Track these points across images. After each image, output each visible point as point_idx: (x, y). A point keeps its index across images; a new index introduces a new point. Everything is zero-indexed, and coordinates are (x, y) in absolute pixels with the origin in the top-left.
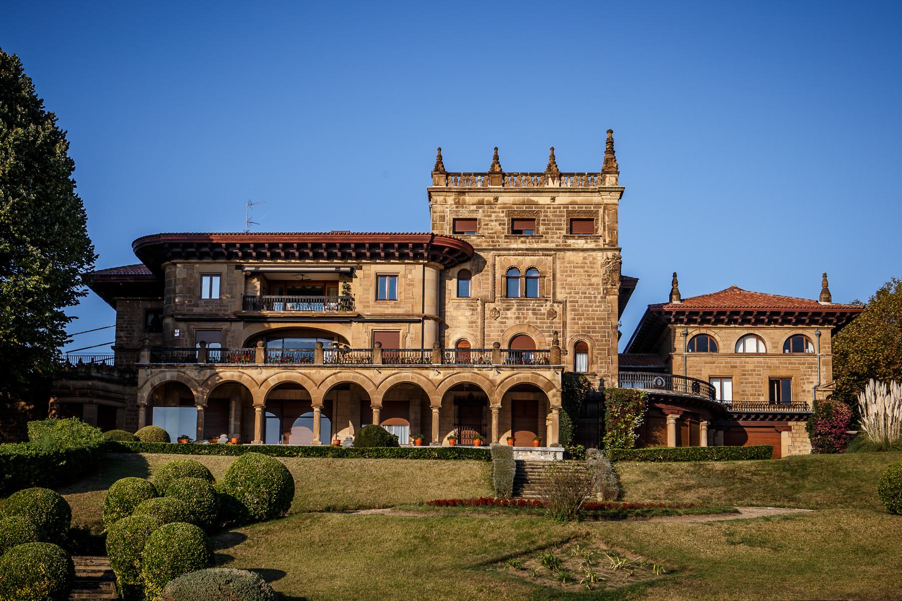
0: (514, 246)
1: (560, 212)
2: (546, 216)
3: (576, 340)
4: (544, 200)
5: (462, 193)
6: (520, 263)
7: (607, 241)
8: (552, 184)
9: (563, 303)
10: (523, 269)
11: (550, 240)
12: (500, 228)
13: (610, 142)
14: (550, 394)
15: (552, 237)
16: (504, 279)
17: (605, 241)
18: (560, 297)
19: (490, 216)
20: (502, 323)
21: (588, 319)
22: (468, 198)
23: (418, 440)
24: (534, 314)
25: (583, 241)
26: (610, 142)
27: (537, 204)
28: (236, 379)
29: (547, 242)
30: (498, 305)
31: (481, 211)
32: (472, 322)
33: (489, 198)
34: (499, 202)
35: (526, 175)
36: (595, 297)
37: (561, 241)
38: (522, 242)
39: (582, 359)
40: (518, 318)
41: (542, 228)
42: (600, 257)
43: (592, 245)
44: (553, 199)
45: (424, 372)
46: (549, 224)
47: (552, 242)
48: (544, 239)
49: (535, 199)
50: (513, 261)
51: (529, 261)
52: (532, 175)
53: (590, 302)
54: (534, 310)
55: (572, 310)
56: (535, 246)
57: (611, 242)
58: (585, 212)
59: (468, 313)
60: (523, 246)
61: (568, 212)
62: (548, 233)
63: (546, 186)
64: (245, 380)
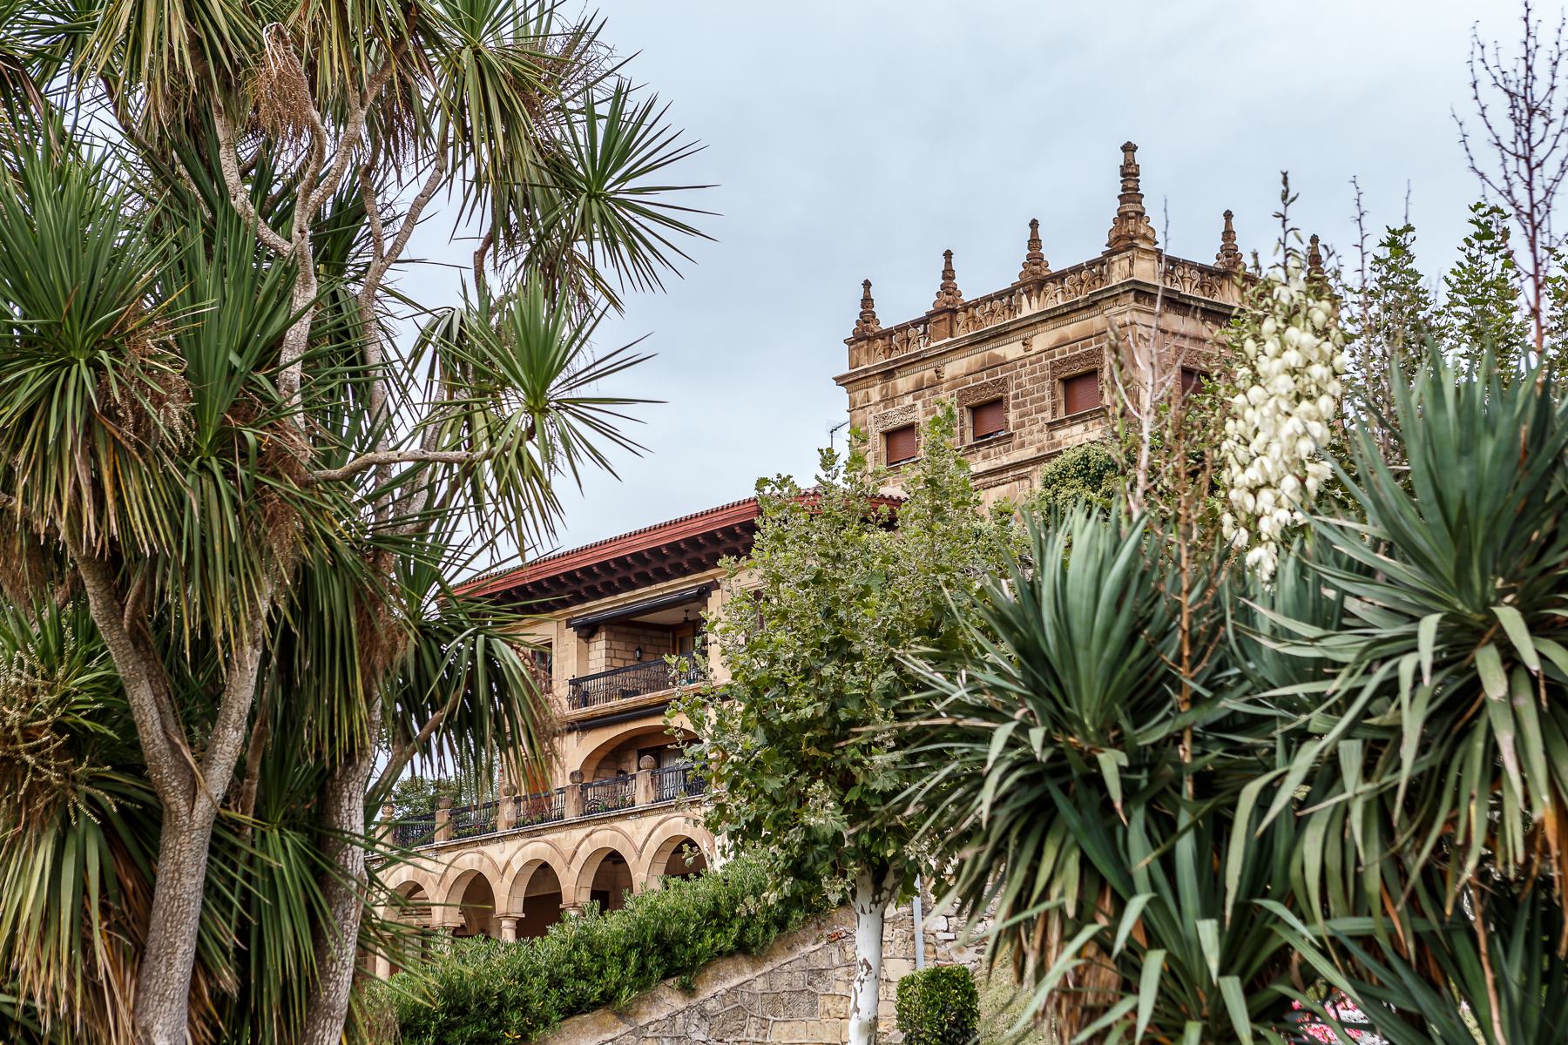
1: (1042, 369)
2: (1019, 386)
4: (1011, 350)
5: (888, 374)
8: (1029, 308)
11: (1027, 439)
13: (1129, 173)
15: (1031, 433)
22: (903, 383)
25: (1081, 427)
26: (1129, 173)
27: (1002, 363)
28: (475, 867)
29: (1022, 445)
31: (919, 403)
33: (929, 373)
34: (947, 376)
37: (1044, 436)
38: (985, 457)
41: (1012, 416)
48: (1017, 441)
49: (998, 351)
52: (999, 296)
56: (1005, 460)
58: (1079, 358)
61: (1054, 367)
62: (1023, 425)
63: (1019, 316)
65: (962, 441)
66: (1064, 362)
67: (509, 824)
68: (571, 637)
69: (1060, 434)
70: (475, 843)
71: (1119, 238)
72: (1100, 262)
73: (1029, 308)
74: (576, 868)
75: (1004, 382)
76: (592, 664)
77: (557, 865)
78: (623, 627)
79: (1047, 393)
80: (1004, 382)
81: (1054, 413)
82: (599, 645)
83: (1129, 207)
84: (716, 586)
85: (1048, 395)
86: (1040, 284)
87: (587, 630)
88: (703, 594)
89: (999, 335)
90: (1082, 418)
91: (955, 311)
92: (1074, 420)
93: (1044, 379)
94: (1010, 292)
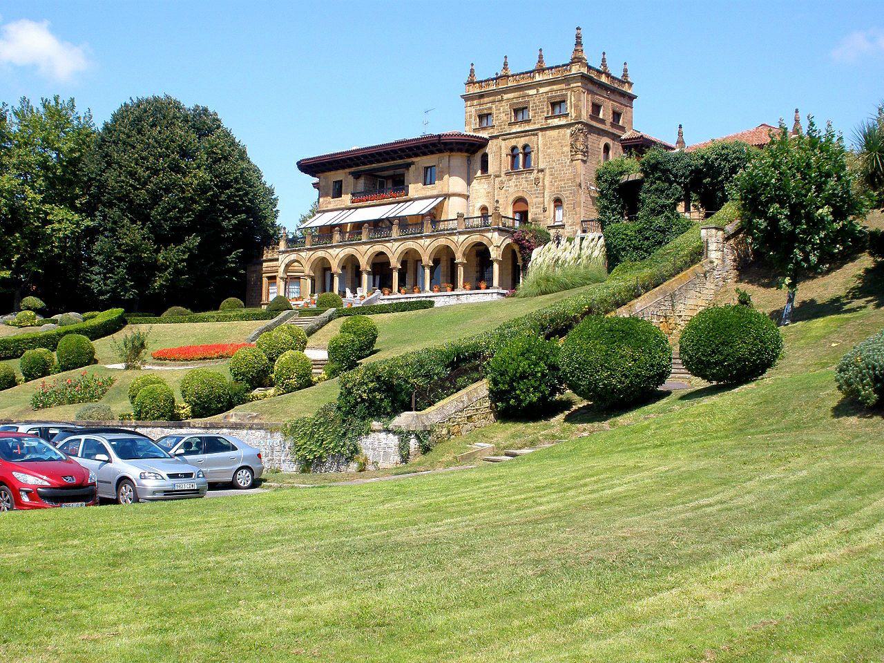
0: (514, 131)
3: (553, 197)
6: (518, 142)
7: (573, 117)
8: (538, 78)
9: (542, 171)
10: (520, 146)
12: (505, 118)
13: (578, 37)
14: (490, 249)
16: (509, 157)
17: (571, 116)
18: (541, 166)
19: (499, 109)
20: (506, 191)
21: (561, 180)
23: (468, 287)
24: (527, 181)
26: (578, 37)
29: (535, 123)
30: (503, 178)
31: (494, 106)
32: (488, 193)
35: (523, 73)
36: (566, 163)
37: (544, 121)
39: (559, 213)
40: (516, 185)
42: (569, 131)
43: (563, 121)
44: (538, 91)
45: (419, 241)
46: (536, 109)
47: (538, 123)
48: (532, 121)
50: (513, 142)
51: (520, 142)
52: (527, 73)
53: (562, 167)
54: (526, 178)
55: (551, 175)
56: (527, 128)
57: (576, 116)
58: (558, 96)
59: (486, 186)
60: (519, 130)
61: (548, 98)
63: (535, 80)
64: (327, 256)
65: (511, 120)
66: (552, 97)
67: (338, 242)
68: (351, 178)
69: (549, 121)
70: (323, 248)
71: (575, 58)
72: (567, 65)
73: (538, 78)
74: (366, 258)
75: (529, 102)
76: (358, 188)
77: (358, 256)
78: (371, 175)
79: (545, 107)
80: (529, 102)
81: (548, 114)
82: (362, 182)
83: (578, 48)
84: (413, 163)
85: (547, 109)
86: (543, 70)
87: (357, 176)
88: (408, 166)
89: (530, 87)
90: (559, 116)
91: (508, 77)
92: (555, 117)
93: (544, 102)
94: (531, 72)
